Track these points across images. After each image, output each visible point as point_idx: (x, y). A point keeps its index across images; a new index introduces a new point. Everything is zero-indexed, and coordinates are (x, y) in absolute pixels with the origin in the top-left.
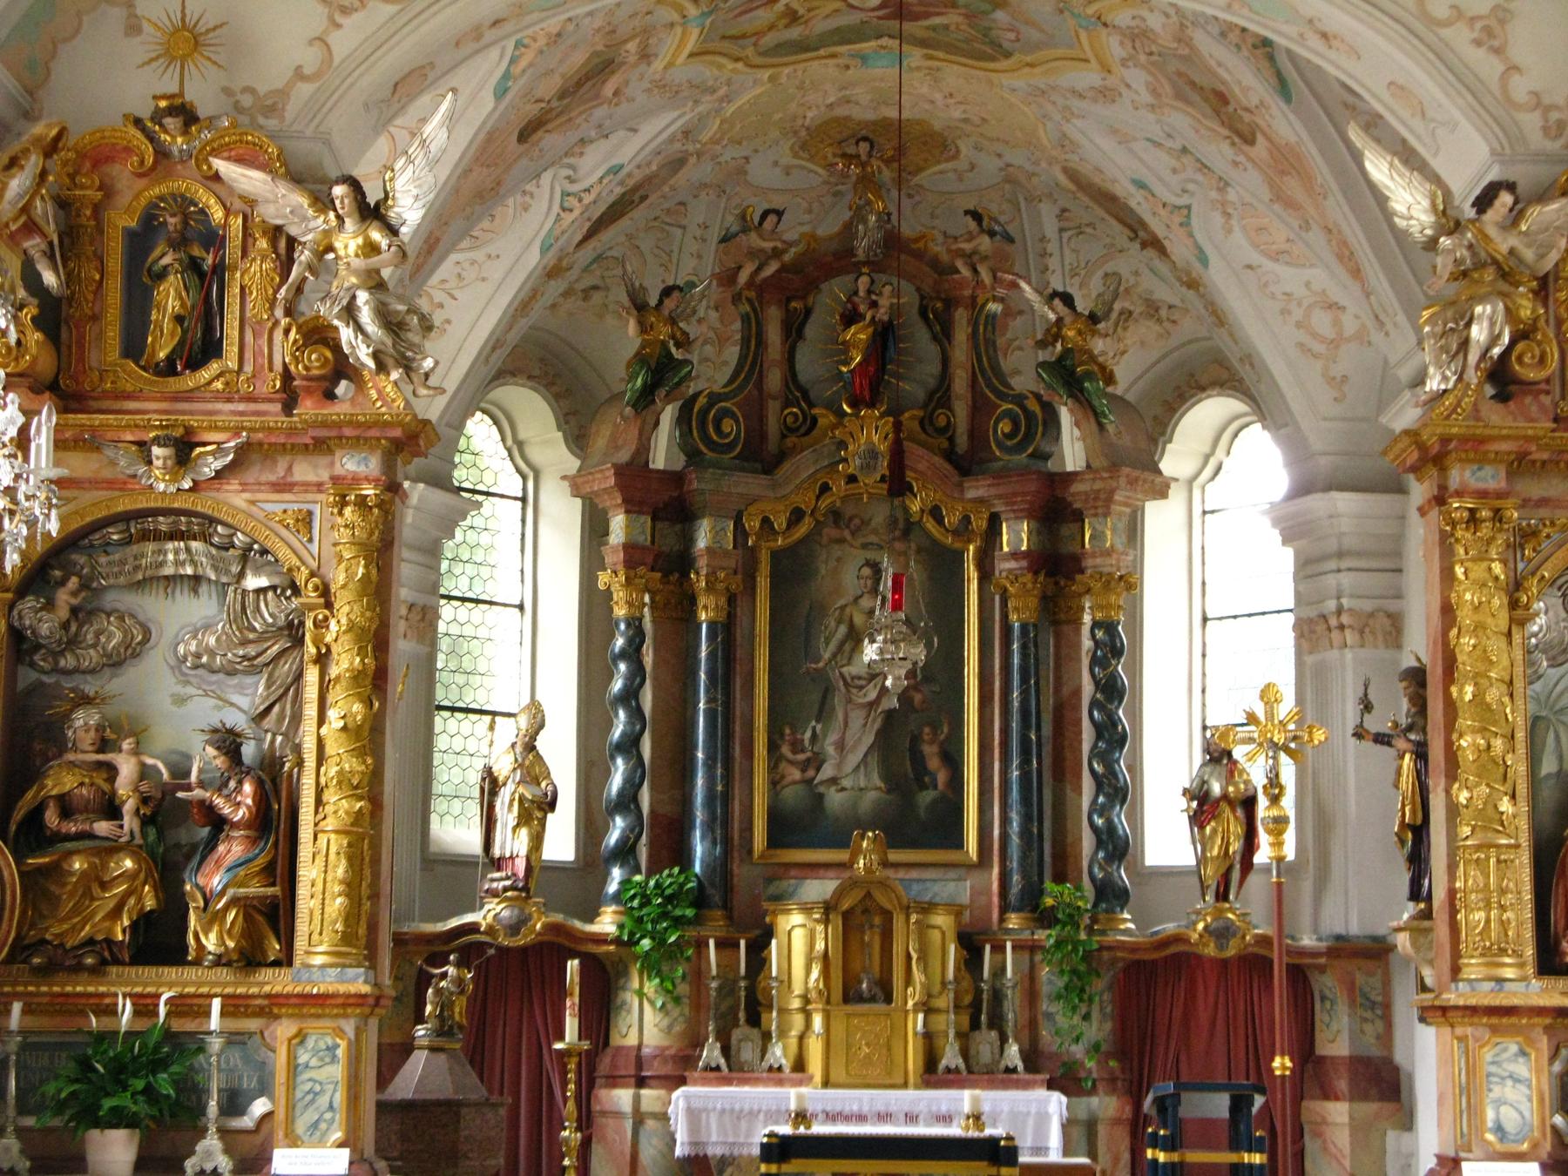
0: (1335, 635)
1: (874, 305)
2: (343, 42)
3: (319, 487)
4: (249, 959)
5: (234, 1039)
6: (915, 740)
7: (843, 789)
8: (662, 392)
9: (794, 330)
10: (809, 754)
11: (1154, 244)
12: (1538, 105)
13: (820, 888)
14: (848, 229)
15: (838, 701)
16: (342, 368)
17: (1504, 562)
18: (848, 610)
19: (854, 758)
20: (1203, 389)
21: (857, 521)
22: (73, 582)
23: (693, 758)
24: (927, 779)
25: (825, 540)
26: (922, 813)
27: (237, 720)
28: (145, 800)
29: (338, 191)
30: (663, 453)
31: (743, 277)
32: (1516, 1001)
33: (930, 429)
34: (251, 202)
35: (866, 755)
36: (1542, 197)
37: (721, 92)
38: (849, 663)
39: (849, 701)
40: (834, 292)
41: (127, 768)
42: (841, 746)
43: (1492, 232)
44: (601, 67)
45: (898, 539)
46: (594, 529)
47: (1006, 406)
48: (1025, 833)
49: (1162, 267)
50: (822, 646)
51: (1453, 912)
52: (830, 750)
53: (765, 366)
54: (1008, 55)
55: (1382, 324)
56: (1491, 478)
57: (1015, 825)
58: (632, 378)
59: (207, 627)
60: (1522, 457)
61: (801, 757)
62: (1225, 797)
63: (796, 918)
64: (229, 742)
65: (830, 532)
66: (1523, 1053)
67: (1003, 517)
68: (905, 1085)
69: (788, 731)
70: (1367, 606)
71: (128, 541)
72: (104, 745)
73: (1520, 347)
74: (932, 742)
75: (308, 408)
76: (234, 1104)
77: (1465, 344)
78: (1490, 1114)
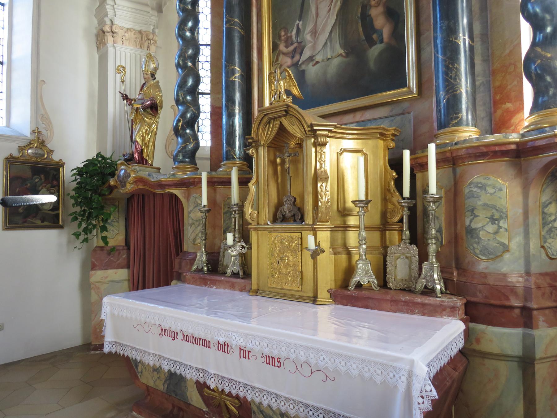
10: (295, 45)
19: (323, 37)
24: (375, 36)
26: (372, 64)
35: (331, 33)
52: (308, 37)
61: (291, 48)
68: (314, 300)
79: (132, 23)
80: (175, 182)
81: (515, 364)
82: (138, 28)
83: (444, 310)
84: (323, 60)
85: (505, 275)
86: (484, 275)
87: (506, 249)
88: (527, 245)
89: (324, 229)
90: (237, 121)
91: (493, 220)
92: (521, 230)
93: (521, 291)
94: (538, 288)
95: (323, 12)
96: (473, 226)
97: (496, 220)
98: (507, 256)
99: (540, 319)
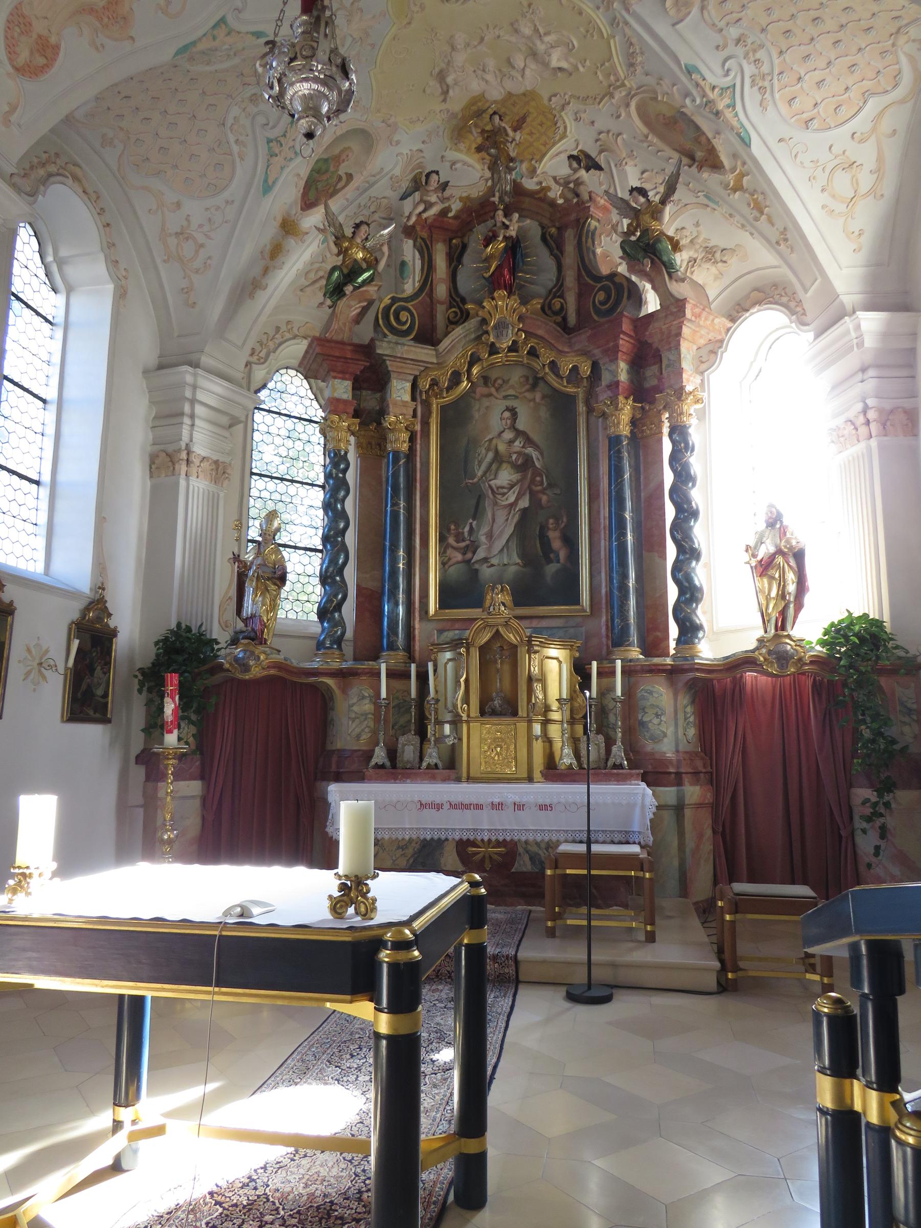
6: (543, 529)
7: (492, 565)
10: (468, 542)
15: (487, 503)
18: (494, 442)
21: (500, 381)
24: (552, 556)
25: (477, 396)
33: (549, 312)
35: (508, 541)
38: (495, 479)
39: (495, 503)
40: (480, 232)
42: (490, 536)
45: (528, 391)
47: (599, 285)
50: (476, 467)
52: (483, 539)
53: (434, 282)
61: (463, 544)
65: (481, 390)
67: (601, 362)
68: (530, 779)
69: (453, 527)
74: (555, 530)
79: (209, 451)
80: (333, 671)
81: (672, 812)
82: (215, 458)
83: (632, 776)
84: (499, 565)
85: (665, 753)
86: (652, 754)
87: (665, 735)
88: (676, 732)
89: (537, 721)
90: (401, 610)
91: (657, 715)
92: (673, 722)
93: (675, 763)
94: (684, 760)
96: (645, 719)
97: (660, 715)
98: (665, 740)
99: (686, 779)
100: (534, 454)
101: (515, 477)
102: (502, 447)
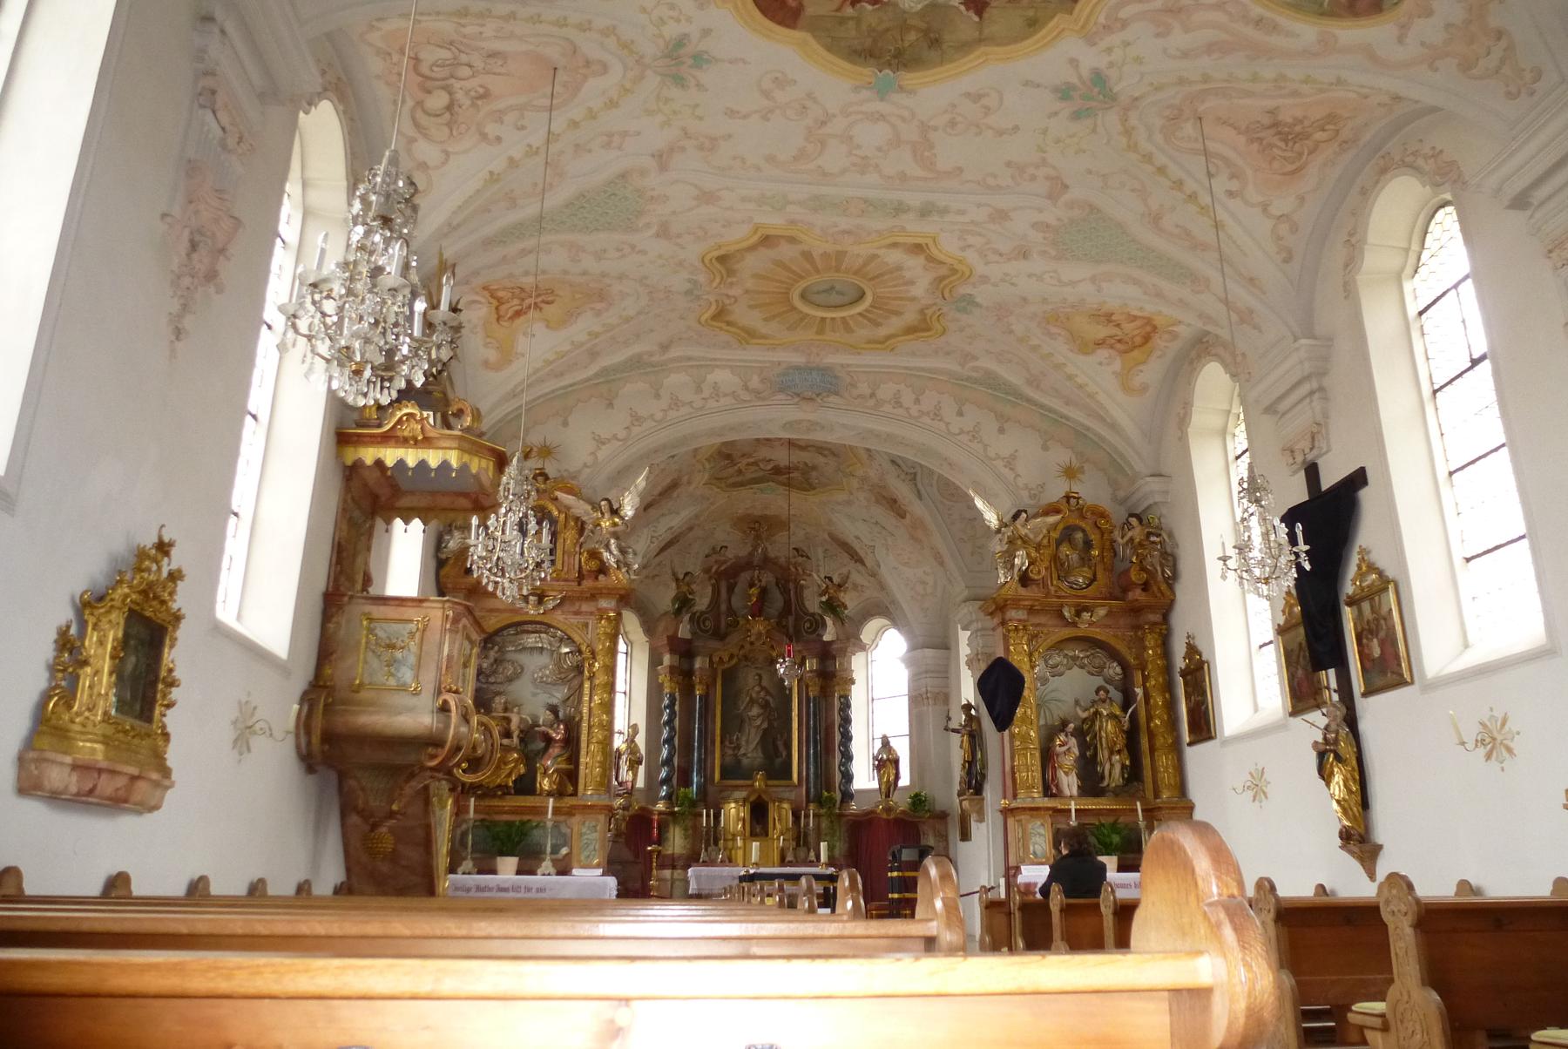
0: (925, 701)
1: (760, 581)
2: (601, 455)
3: (592, 613)
4: (559, 793)
5: (556, 825)
8: (685, 609)
9: (731, 589)
11: (860, 561)
12: (1027, 488)
13: (743, 794)
14: (751, 554)
16: (603, 569)
17: (1028, 645)
19: (752, 746)
20: (872, 616)
22: (496, 648)
23: (693, 746)
27: (555, 701)
28: (521, 731)
29: (603, 503)
30: (684, 631)
31: (713, 570)
32: (1041, 805)
34: (568, 508)
36: (1035, 516)
37: (712, 500)
39: (750, 725)
40: (745, 577)
41: (515, 720)
42: (747, 741)
43: (1019, 527)
44: (674, 485)
46: (654, 662)
48: (816, 774)
49: (860, 567)
51: (1013, 773)
54: (814, 489)
55: (950, 581)
56: (1022, 615)
57: (812, 770)
58: (673, 605)
59: (546, 667)
60: (1032, 606)
62: (888, 759)
63: (733, 805)
64: (554, 710)
65: (745, 663)
66: (1042, 825)
70: (937, 690)
71: (517, 634)
72: (506, 710)
73: (1031, 567)
75: (588, 583)
76: (555, 850)
77: (1013, 565)
78: (1031, 848)
95: (752, 735)
100: (771, 700)
101: (761, 711)
102: (754, 695)
